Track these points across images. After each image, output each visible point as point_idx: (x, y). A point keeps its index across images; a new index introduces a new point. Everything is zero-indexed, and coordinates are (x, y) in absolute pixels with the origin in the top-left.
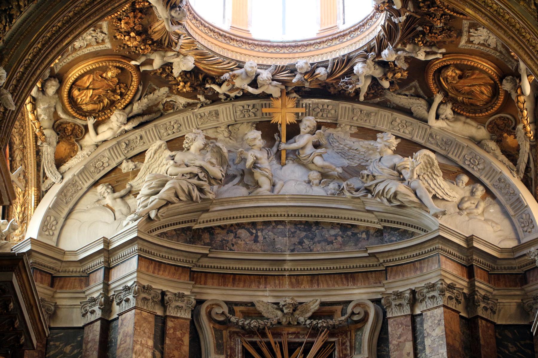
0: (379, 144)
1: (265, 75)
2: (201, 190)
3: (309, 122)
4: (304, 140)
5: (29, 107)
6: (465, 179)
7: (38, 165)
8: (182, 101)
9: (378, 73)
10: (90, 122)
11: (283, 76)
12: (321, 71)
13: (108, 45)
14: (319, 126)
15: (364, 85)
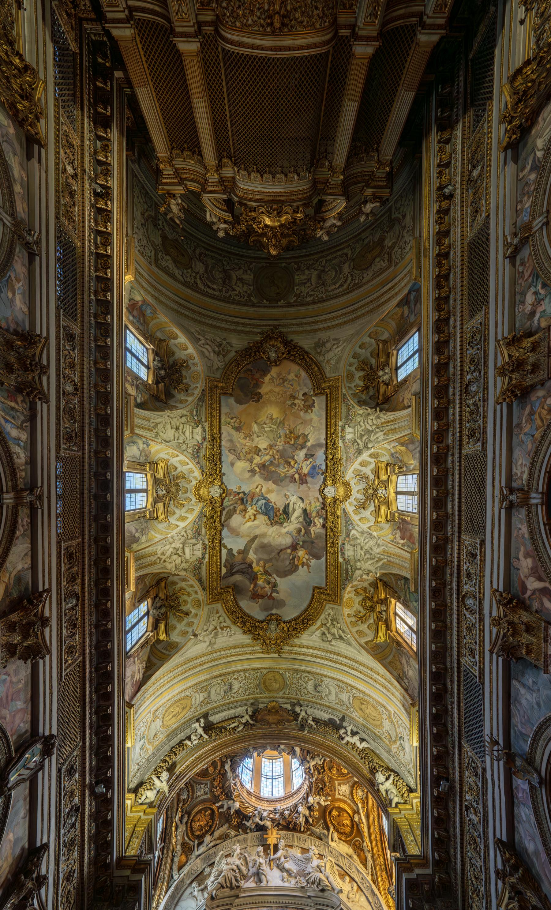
0: (311, 853)
1: (265, 814)
2: (236, 880)
3: (282, 843)
4: (280, 853)
5: (174, 829)
6: (348, 878)
7: (171, 868)
8: (233, 833)
9: (307, 813)
10: (196, 842)
11: (272, 816)
12: (286, 813)
13: (209, 796)
14: (286, 846)
15: (302, 819)
